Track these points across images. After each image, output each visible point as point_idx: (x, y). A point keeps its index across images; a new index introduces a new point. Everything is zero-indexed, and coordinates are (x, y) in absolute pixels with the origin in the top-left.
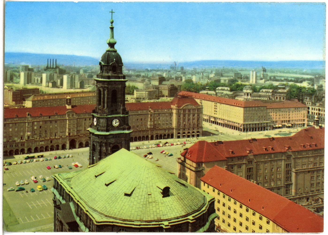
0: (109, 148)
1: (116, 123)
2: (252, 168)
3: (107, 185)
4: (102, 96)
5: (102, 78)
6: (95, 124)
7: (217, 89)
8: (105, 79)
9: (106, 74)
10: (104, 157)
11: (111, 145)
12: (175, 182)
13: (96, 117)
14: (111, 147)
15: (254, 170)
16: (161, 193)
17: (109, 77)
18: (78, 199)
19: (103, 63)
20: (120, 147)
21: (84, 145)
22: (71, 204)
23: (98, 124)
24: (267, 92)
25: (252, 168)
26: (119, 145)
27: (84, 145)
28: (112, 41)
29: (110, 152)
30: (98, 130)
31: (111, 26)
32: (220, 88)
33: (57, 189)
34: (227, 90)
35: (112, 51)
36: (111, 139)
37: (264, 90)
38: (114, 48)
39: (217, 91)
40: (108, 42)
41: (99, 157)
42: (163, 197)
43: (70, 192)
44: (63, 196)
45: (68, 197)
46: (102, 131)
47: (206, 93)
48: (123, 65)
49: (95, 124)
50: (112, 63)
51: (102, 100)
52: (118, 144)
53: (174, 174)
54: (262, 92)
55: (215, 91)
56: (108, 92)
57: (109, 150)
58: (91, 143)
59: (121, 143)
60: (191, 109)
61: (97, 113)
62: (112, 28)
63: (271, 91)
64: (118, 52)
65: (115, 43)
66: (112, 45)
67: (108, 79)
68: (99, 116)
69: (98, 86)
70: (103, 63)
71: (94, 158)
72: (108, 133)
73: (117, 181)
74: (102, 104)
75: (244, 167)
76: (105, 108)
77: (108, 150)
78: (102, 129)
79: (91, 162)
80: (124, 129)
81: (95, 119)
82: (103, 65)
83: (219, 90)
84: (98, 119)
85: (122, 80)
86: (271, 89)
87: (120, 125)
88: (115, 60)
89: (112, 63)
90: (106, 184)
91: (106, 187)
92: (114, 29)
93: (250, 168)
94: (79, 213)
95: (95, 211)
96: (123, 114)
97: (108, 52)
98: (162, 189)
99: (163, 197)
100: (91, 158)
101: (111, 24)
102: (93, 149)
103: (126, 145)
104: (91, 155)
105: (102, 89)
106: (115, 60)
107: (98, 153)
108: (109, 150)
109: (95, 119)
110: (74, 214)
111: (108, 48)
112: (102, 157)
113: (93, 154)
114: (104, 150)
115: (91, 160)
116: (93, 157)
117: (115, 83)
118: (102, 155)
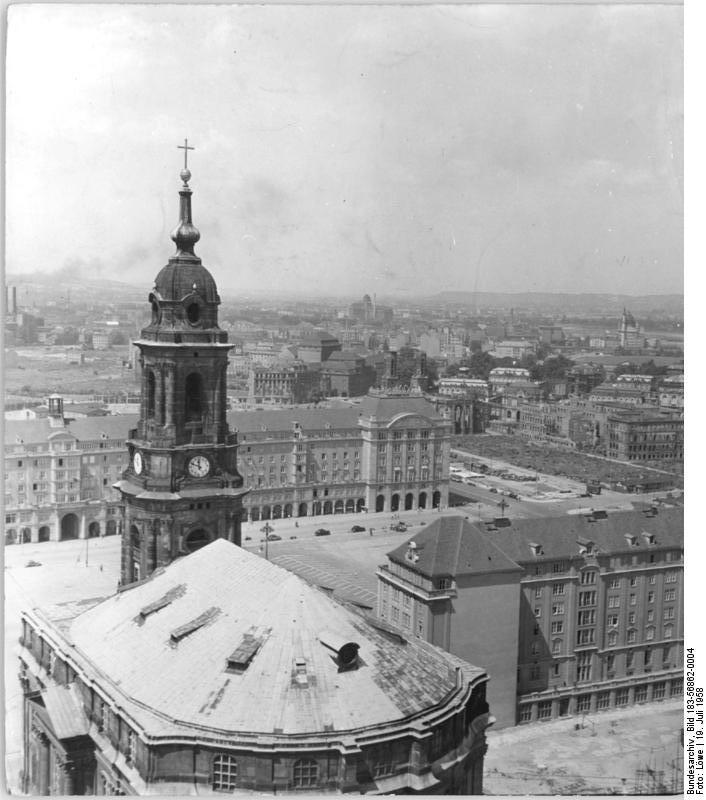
0: (181, 539)
1: (201, 467)
2: (594, 592)
4: (158, 390)
5: (156, 340)
6: (138, 469)
7: (492, 372)
8: (167, 341)
9: (171, 329)
10: (165, 563)
11: (186, 529)
13: (139, 450)
15: (599, 598)
16: (333, 658)
17: (178, 338)
20: (212, 535)
21: (103, 531)
23: (147, 468)
24: (637, 383)
25: (594, 592)
26: (209, 530)
27: (103, 531)
28: (185, 231)
29: (183, 549)
30: (146, 487)
31: (182, 189)
32: (501, 370)
34: (523, 376)
35: (186, 261)
36: (184, 513)
37: (628, 377)
38: (192, 253)
39: (492, 380)
40: (175, 234)
41: (150, 561)
42: (340, 671)
46: (159, 489)
47: (459, 384)
48: (219, 303)
49: (138, 469)
50: (187, 295)
51: (157, 403)
52: (205, 528)
53: (371, 609)
54: (624, 380)
55: (486, 379)
56: (175, 378)
58: (127, 522)
59: (215, 523)
60: (416, 430)
62: (186, 196)
63: (648, 378)
66: (186, 243)
67: (176, 342)
68: (148, 446)
69: (146, 362)
70: (160, 297)
71: (137, 566)
72: (176, 496)
74: (158, 413)
75: (569, 589)
76: (167, 425)
77: (177, 543)
78: (159, 483)
79: (127, 576)
80: (224, 485)
81: (138, 457)
82: (160, 302)
83: (498, 376)
84: (147, 454)
85: (219, 345)
86: (647, 373)
87: (212, 473)
88: (195, 286)
89: (187, 295)
93: (588, 594)
96: (219, 442)
97: (175, 265)
99: (340, 671)
100: (127, 564)
101: (183, 183)
102: (134, 540)
104: (128, 557)
105: (157, 374)
107: (146, 551)
108: (180, 545)
109: (138, 457)
111: (173, 251)
112: (158, 561)
113: (132, 555)
114: (165, 544)
115: (127, 571)
116: (133, 562)
117: (196, 355)
118: (157, 559)
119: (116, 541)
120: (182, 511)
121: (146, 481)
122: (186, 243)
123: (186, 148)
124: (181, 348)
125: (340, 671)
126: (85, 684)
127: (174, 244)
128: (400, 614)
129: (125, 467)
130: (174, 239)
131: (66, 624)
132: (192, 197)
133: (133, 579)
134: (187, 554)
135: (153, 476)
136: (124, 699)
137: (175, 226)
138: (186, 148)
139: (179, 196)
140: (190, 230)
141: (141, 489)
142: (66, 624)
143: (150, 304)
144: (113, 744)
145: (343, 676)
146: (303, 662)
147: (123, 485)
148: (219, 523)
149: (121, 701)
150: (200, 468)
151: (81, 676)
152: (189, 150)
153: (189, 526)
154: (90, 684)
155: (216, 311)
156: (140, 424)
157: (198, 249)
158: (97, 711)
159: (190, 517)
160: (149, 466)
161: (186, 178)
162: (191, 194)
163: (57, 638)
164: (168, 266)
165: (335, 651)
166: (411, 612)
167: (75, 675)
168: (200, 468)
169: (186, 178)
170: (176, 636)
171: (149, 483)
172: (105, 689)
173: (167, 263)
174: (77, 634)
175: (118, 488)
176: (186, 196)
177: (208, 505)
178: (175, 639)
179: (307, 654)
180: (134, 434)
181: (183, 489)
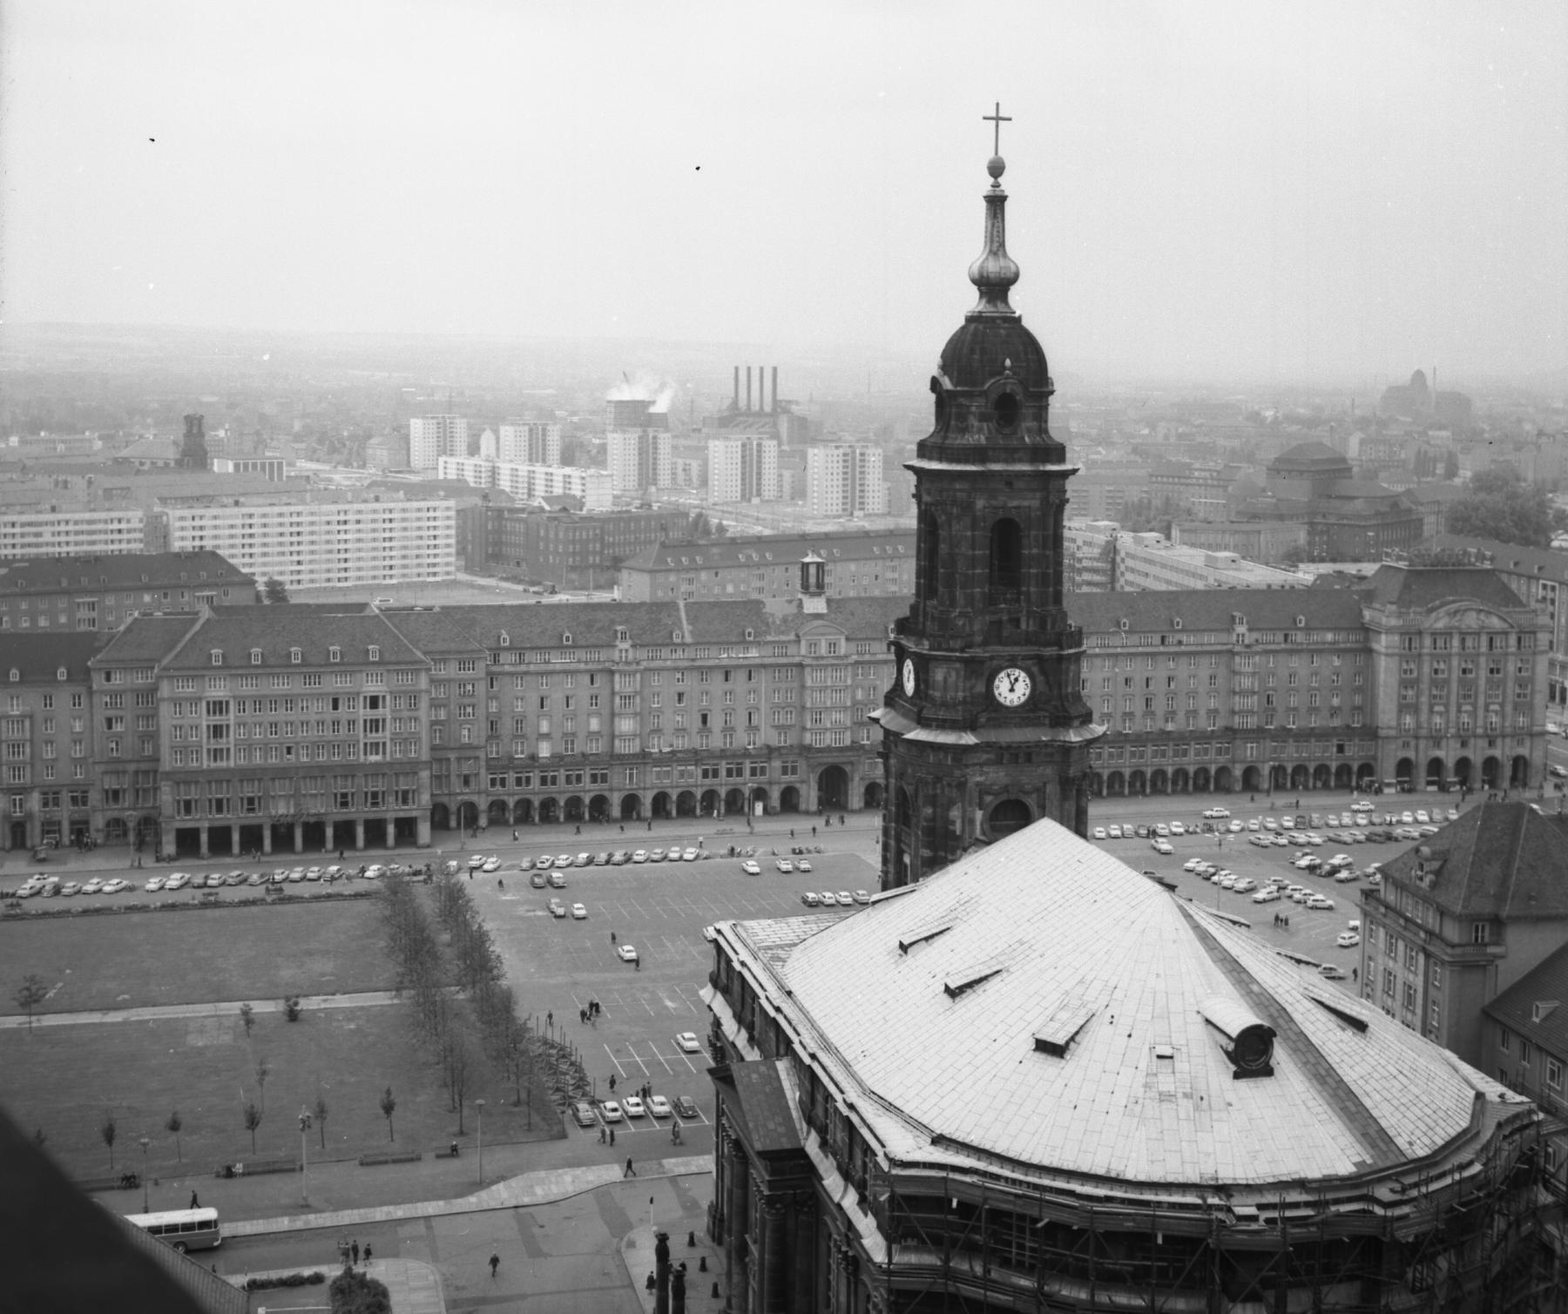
0: (979, 815)
3: (953, 993)
6: (909, 687)
11: (988, 799)
12: (1311, 1005)
14: (990, 810)
16: (1227, 1053)
18: (813, 1047)
19: (947, 384)
20: (1035, 810)
22: (782, 1066)
26: (1031, 802)
28: (993, 267)
29: (984, 833)
30: (923, 722)
33: (725, 991)
38: (1005, 299)
40: (975, 269)
42: (1237, 1076)
43: (778, 1009)
44: (750, 1028)
45: (773, 1037)
46: (943, 725)
49: (909, 687)
50: (994, 374)
57: (978, 823)
59: (1040, 791)
61: (921, 635)
62: (996, 203)
64: (1026, 323)
65: (1014, 279)
66: (995, 287)
68: (924, 648)
69: (926, 498)
70: (947, 384)
71: (907, 859)
72: (969, 739)
73: (1004, 974)
77: (972, 821)
78: (942, 714)
81: (909, 666)
82: (948, 391)
89: (994, 374)
90: (947, 989)
91: (946, 998)
92: (1009, 206)
94: (820, 1111)
95: (890, 1107)
97: (973, 326)
98: (1234, 1035)
99: (1237, 1076)
100: (891, 855)
101: (992, 180)
103: (1071, 806)
104: (892, 843)
106: (1008, 362)
108: (978, 823)
109: (909, 666)
110: (795, 1114)
113: (898, 840)
115: (891, 869)
116: (900, 853)
118: (941, 849)
119: (876, 821)
120: (981, 765)
121: (920, 711)
122: (995, 287)
123: (998, 119)
124: (982, 473)
125: (1237, 1076)
126: (801, 1061)
127: (975, 288)
128: (1399, 986)
129: (886, 685)
130: (974, 282)
131: (781, 953)
132: (1007, 204)
133: (900, 882)
134: (989, 843)
135: (932, 700)
136: (859, 1091)
137: (972, 252)
138: (998, 119)
139: (984, 204)
140: (1002, 262)
141: (914, 725)
142: (781, 953)
143: (933, 396)
144: (839, 1168)
145: (1243, 1084)
146: (1168, 1052)
147: (884, 715)
148: (1049, 788)
149: (853, 1097)
150: (1012, 690)
151: (797, 1047)
152: (993, 114)
153: (996, 794)
154: (807, 1060)
155: (1046, 407)
156: (914, 608)
157: (1019, 300)
158: (820, 1111)
159: (997, 776)
160: (926, 682)
161: (996, 169)
162: (1004, 198)
163: (763, 977)
164: (963, 328)
165: (1229, 1037)
166: (1419, 982)
167: (789, 1042)
168: (1012, 690)
169: (996, 169)
170: (952, 986)
171: (925, 713)
172: (831, 1071)
173: (962, 322)
174: (796, 973)
175: (876, 721)
176: (996, 203)
177: (1029, 759)
178: (953, 993)
179: (1178, 1039)
180: (903, 626)
181: (983, 727)
